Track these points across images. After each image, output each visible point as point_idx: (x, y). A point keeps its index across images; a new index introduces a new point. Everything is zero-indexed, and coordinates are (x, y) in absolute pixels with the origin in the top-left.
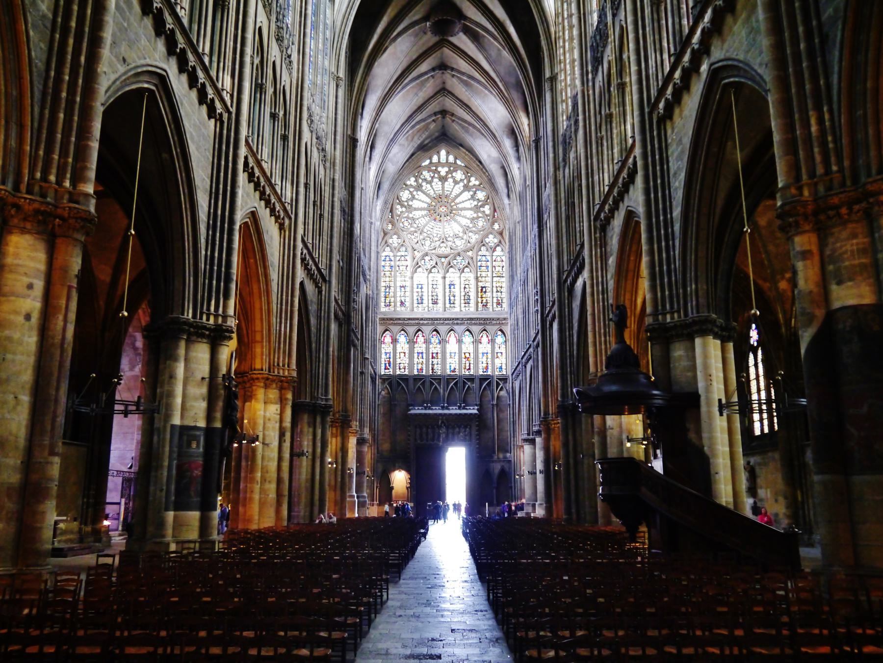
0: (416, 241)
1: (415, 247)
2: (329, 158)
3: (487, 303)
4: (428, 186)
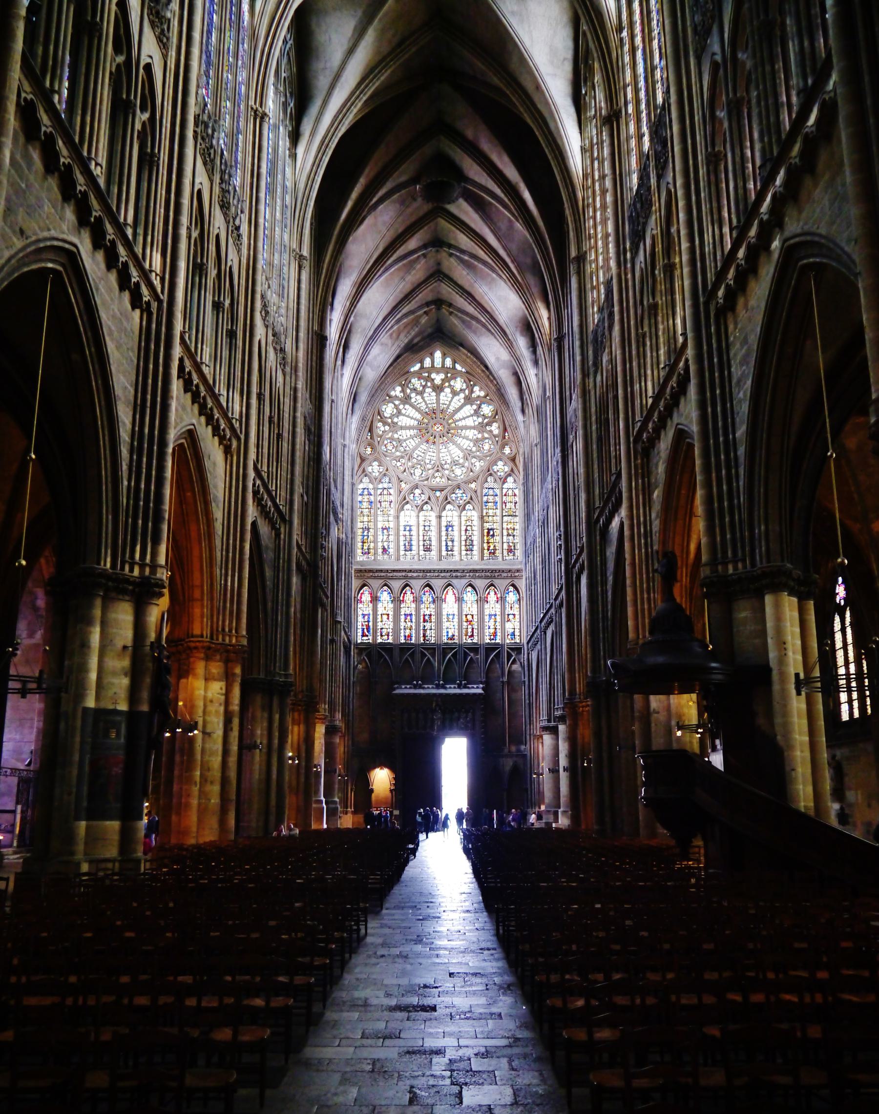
0: (402, 468)
1: (401, 476)
2: (290, 361)
3: (495, 550)
4: (419, 397)
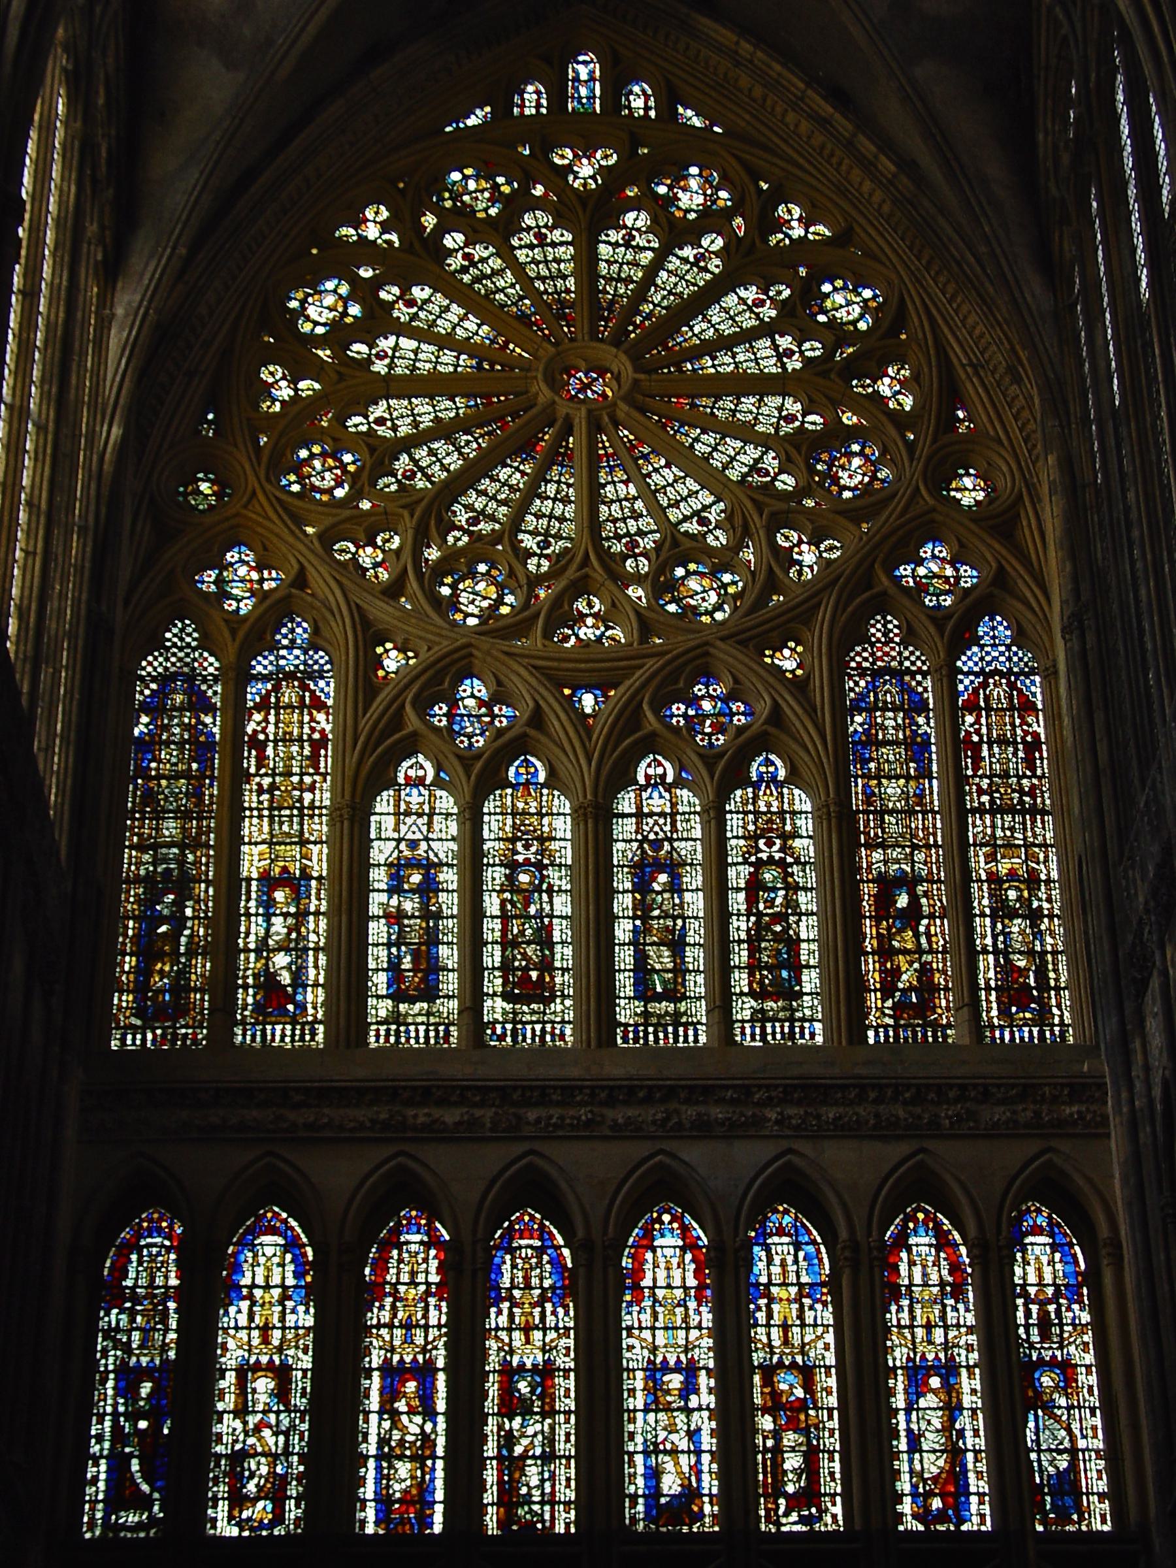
1: (379, 611)
4: (479, 251)
